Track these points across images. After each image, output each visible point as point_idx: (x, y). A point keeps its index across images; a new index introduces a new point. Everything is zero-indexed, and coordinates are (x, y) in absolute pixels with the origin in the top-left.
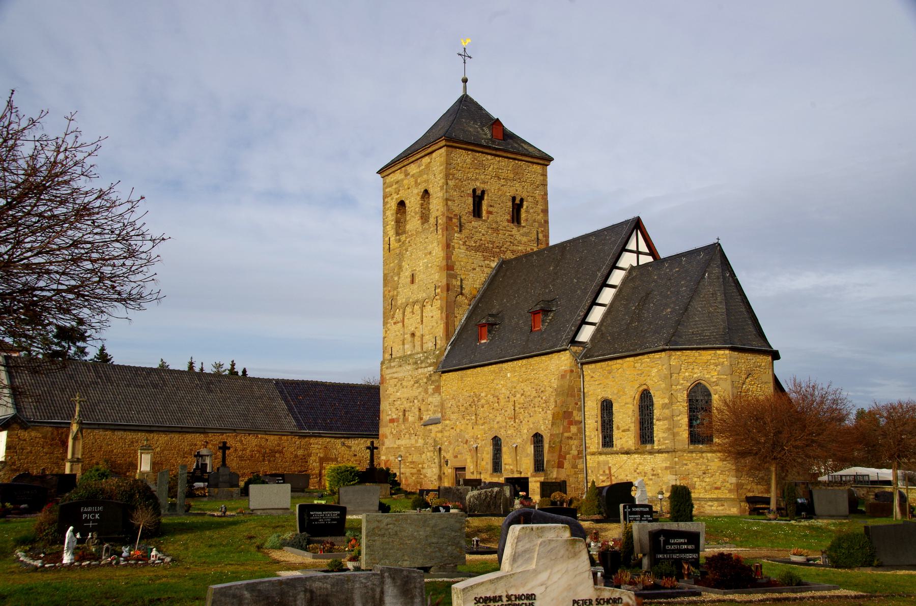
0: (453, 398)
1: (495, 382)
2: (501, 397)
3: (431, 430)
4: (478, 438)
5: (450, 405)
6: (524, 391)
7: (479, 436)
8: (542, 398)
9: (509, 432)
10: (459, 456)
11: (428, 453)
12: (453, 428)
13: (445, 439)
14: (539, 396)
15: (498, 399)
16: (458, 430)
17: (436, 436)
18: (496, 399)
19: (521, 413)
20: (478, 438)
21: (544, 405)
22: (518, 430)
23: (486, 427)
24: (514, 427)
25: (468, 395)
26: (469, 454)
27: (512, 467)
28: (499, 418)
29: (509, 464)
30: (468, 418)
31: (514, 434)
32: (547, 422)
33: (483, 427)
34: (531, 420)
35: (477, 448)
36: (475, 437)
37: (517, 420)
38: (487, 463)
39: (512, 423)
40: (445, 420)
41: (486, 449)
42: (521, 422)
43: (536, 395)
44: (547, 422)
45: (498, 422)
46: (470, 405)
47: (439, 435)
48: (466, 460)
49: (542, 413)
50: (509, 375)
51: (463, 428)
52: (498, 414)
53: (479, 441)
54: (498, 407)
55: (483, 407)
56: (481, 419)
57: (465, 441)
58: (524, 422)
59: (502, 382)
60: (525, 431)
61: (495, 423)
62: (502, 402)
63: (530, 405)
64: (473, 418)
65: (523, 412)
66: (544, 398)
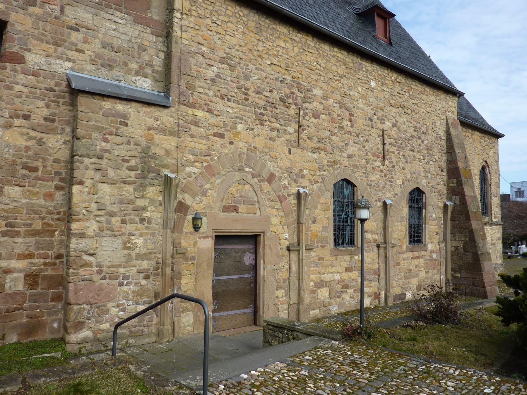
0: (223, 61)
1: (344, 80)
2: (358, 113)
3: (124, 116)
4: (303, 177)
5: (210, 73)
6: (396, 121)
7: (306, 172)
8: (423, 142)
9: (373, 178)
10: (242, 208)
11: (105, 188)
12: (221, 136)
13: (191, 157)
14: (419, 138)
15: (352, 115)
16: (242, 146)
17: (151, 140)
18: (347, 113)
19: (393, 152)
20: (303, 177)
21: (426, 152)
22: (388, 177)
23: (324, 158)
24: (382, 171)
25: (277, 75)
26: (278, 205)
27: (376, 237)
28: (352, 149)
29: (372, 232)
30: (276, 125)
31: (382, 184)
32: (429, 176)
33: (315, 156)
34: (408, 167)
35: (299, 194)
36: (295, 171)
37: (387, 162)
38: (324, 229)
39: (379, 164)
40: (192, 106)
41: (322, 200)
42: (393, 167)
43: (415, 134)
44: (429, 176)
45: (350, 156)
46: (283, 100)
47: (170, 142)
48: (268, 219)
49: (423, 161)
50: (373, 84)
51: (259, 142)
52: (351, 142)
53: (305, 182)
54: (351, 130)
55: (316, 116)
56: (310, 138)
57: (265, 174)
58: (397, 167)
59: (360, 89)
60: (400, 182)
61: (345, 155)
62: (360, 123)
63: (406, 146)
64: (291, 130)
65: (396, 153)
66: (426, 142)
